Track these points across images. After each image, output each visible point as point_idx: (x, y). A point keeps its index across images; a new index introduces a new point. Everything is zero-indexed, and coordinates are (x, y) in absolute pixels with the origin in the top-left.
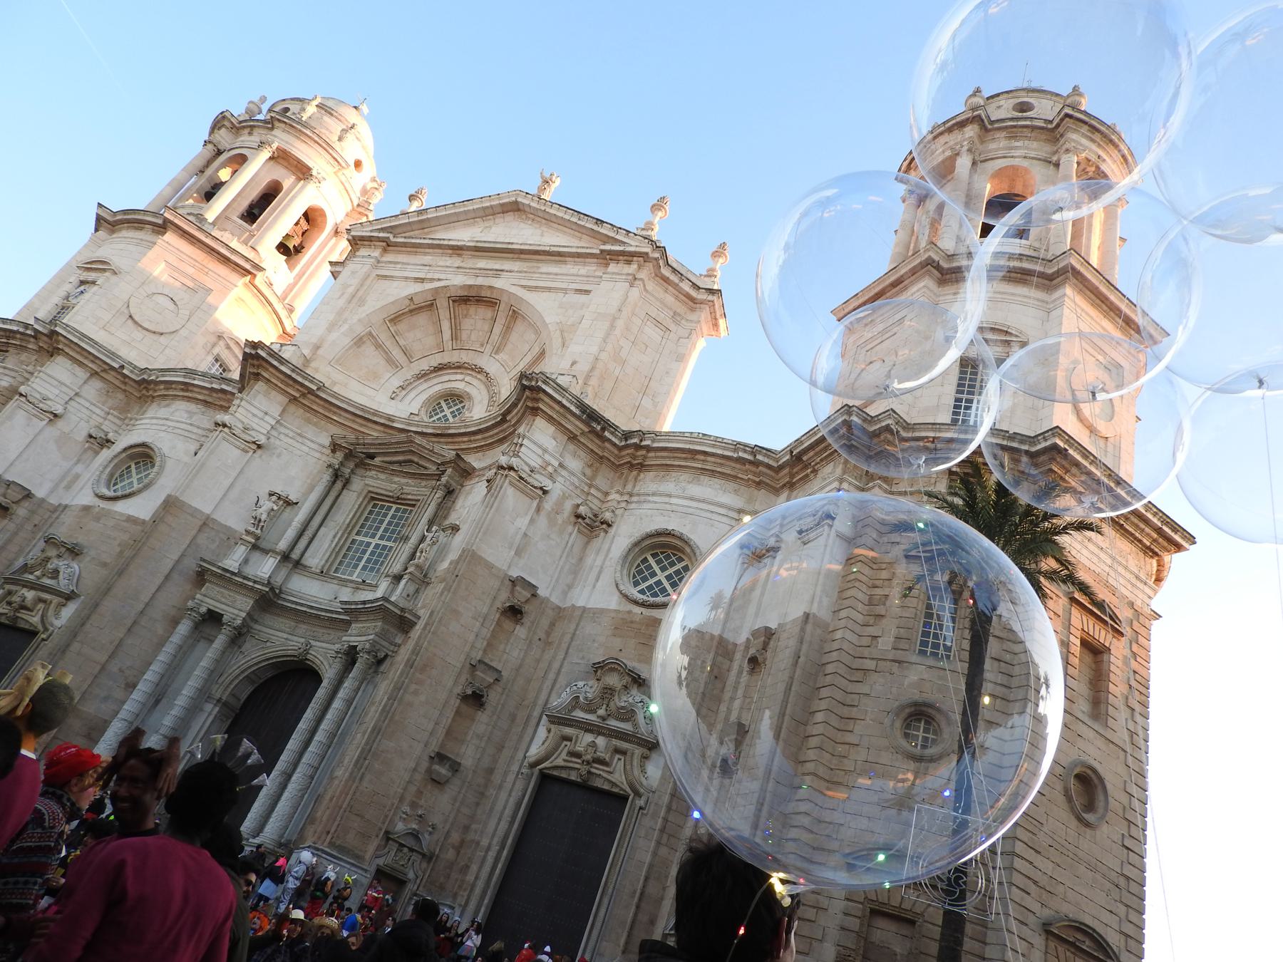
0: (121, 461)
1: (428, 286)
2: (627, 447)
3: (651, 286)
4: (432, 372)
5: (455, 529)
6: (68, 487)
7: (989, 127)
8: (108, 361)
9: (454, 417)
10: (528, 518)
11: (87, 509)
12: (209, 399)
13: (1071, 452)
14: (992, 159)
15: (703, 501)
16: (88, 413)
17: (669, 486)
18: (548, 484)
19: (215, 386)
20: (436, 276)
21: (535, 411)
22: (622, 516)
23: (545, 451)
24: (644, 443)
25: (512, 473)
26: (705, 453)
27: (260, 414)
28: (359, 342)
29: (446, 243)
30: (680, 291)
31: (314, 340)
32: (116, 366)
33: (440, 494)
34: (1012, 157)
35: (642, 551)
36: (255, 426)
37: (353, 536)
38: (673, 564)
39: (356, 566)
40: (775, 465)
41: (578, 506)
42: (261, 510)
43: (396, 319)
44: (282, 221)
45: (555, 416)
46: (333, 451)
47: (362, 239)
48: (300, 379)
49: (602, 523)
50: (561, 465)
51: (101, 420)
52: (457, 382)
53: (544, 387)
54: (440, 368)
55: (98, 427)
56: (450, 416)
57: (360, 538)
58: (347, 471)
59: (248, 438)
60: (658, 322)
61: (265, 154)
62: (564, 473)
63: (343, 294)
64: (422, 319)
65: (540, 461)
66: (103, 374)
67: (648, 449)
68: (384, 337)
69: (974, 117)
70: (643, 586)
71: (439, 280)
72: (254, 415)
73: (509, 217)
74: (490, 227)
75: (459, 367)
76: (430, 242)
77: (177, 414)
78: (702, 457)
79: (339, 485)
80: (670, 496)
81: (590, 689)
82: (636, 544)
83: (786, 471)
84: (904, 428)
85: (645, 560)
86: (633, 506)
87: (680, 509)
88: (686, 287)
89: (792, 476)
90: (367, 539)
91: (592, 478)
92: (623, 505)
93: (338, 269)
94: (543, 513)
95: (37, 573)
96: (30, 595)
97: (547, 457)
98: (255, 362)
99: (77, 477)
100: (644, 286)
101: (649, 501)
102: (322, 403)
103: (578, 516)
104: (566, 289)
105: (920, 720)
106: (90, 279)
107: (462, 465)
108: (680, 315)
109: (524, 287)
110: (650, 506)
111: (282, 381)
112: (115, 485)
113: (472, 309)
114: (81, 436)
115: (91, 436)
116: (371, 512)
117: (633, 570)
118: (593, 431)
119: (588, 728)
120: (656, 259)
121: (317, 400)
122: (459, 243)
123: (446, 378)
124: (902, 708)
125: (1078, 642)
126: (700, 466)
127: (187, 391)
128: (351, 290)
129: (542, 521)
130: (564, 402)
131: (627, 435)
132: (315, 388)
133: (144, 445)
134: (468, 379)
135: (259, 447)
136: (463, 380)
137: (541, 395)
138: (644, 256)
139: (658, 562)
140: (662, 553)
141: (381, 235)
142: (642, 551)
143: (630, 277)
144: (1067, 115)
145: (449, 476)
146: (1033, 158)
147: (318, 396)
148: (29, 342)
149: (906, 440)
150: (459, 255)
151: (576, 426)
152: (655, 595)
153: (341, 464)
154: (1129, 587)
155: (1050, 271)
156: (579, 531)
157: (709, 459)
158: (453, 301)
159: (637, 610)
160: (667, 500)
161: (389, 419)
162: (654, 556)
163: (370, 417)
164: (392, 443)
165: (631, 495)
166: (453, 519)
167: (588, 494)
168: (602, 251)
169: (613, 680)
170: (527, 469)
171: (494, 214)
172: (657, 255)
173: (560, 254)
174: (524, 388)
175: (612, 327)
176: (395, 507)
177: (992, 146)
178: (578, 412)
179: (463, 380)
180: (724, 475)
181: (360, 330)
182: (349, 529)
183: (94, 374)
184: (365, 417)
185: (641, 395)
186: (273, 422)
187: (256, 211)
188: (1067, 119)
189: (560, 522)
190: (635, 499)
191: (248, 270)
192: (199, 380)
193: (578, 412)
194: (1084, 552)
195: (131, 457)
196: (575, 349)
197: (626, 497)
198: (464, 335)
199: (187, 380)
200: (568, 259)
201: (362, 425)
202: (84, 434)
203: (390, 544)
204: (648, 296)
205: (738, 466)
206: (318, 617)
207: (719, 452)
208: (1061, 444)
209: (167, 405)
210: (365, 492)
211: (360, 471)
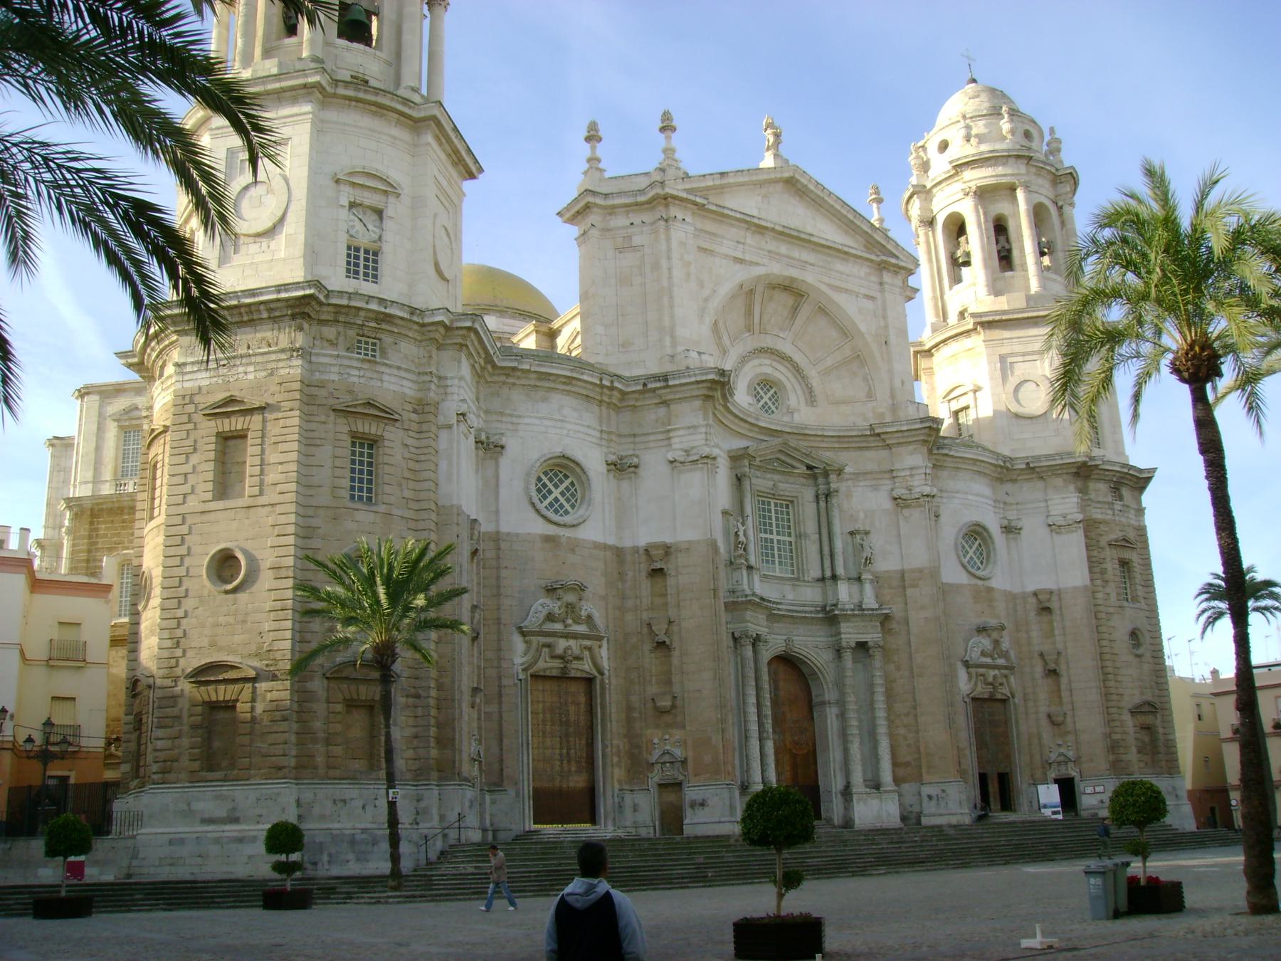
11: (548, 539)
20: (754, 259)
26: (983, 461)
29: (756, 221)
39: (773, 562)
63: (688, 275)
71: (757, 264)
80: (966, 493)
86: (945, 500)
89: (1019, 475)
96: (572, 643)
106: (367, 202)
109: (829, 286)
134: (774, 364)
148: (410, 329)
159: (980, 583)
161: (757, 419)
169: (995, 635)
173: (846, 253)
176: (772, 502)
179: (771, 366)
192: (589, 375)
199: (575, 375)
206: (792, 617)
209: (545, 400)
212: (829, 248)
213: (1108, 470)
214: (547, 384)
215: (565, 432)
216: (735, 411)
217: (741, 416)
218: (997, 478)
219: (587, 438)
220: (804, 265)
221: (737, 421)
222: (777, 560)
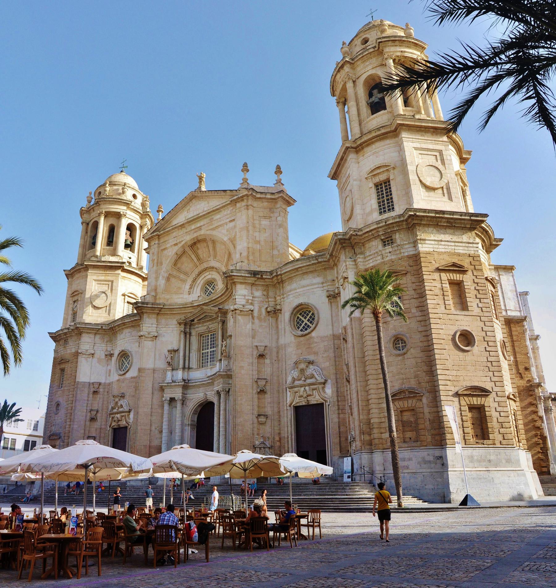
0: (119, 360)
1: (180, 245)
2: (273, 277)
3: (255, 204)
4: (198, 276)
5: (231, 336)
6: (109, 375)
7: (353, 62)
8: (97, 327)
9: (213, 290)
10: (251, 323)
12: (133, 325)
13: (418, 214)
14: (360, 76)
15: (308, 286)
16: (101, 347)
17: (294, 285)
18: (251, 307)
19: (132, 320)
20: (181, 240)
21: (234, 283)
22: (284, 304)
23: (245, 296)
24: (279, 273)
25: (237, 311)
27: (150, 325)
28: (168, 279)
29: (177, 225)
30: (268, 199)
31: (153, 288)
32: (100, 327)
33: (220, 325)
34: (368, 71)
35: (295, 315)
36: (151, 330)
37: (202, 352)
38: (308, 315)
39: (208, 362)
40: (326, 260)
41: (267, 308)
42: (168, 359)
43: (175, 264)
44: (122, 235)
45: (242, 281)
46: (180, 325)
47: (149, 238)
48: (156, 306)
49: (278, 310)
50: (253, 297)
51: (106, 348)
52: (208, 276)
53: (232, 274)
54: (200, 274)
55: (107, 351)
56: (212, 291)
57: (204, 351)
58: (188, 330)
59: (151, 336)
60: (265, 217)
61: (102, 219)
62: (256, 299)
64: (184, 259)
65: (245, 301)
66: (98, 332)
67: (281, 275)
68: (175, 273)
69: (344, 63)
70: (301, 327)
71: (182, 241)
72: (149, 327)
73: (194, 201)
74: (189, 209)
75: (205, 270)
76: (171, 228)
77: (126, 335)
78: (300, 269)
79: (188, 336)
80: (296, 289)
81: (295, 374)
82: (292, 313)
83: (331, 260)
84: (358, 231)
85: (298, 317)
87: (301, 293)
88: (269, 196)
90: (206, 351)
91: (268, 294)
92: (282, 300)
93: (148, 250)
94: (255, 318)
95: (117, 408)
97: (247, 298)
98: (140, 309)
99: (110, 371)
100: (253, 206)
101: (290, 295)
102: (167, 310)
103: (269, 312)
104: (226, 223)
105: (399, 341)
107: (223, 311)
108: (272, 208)
109: (212, 229)
110: (291, 296)
111: (151, 310)
112: (122, 368)
113: (198, 245)
114: (103, 357)
115: (106, 355)
116: (203, 340)
117: (296, 323)
118: (258, 278)
119: (301, 386)
120: (252, 194)
121: (165, 310)
122: (182, 223)
123: (203, 276)
124: (391, 339)
125: (448, 285)
126: (301, 273)
127: (125, 325)
128: (155, 261)
129: (256, 321)
130: (243, 275)
131: (271, 273)
132: (162, 306)
133: (123, 351)
134: (211, 272)
135: (156, 337)
136: (209, 274)
137: (233, 277)
138: (247, 195)
139: (303, 316)
140: (303, 312)
141: (155, 234)
142: (295, 315)
143: (245, 207)
144: (379, 42)
145: (220, 317)
146: (376, 67)
147: (165, 308)
149: (361, 235)
150: (184, 227)
151: (251, 280)
152: (306, 329)
153: (185, 328)
154: (466, 249)
155: (393, 128)
156: (271, 317)
157: (303, 268)
158: (191, 246)
160: (295, 291)
161: (192, 304)
162: (300, 314)
163: (185, 306)
164: (197, 313)
165: (283, 295)
166: (229, 334)
167: (269, 301)
168: (231, 201)
170: (241, 306)
171: (188, 203)
172: (250, 193)
173: (217, 209)
174: (226, 277)
175: (248, 231)
176: (210, 334)
177: (359, 69)
178: (249, 275)
179: (209, 274)
180: (311, 272)
181: (166, 275)
182: (199, 350)
183: (95, 334)
184: (184, 307)
185: (272, 251)
186: (156, 326)
187: (111, 240)
188: (380, 44)
189: (263, 318)
190: (285, 296)
191: (120, 267)
193: (249, 275)
194: (440, 247)
195: (121, 357)
196: (239, 247)
197: (282, 297)
198: (201, 256)
199: (123, 322)
200: (221, 209)
201: (184, 310)
202: (104, 355)
203: (214, 349)
204: (256, 209)
205: (314, 266)
207: (305, 265)
208: (412, 213)
209: (122, 333)
210: (197, 334)
211: (192, 327)
212: (209, 213)
213: (367, 232)
214: (120, 328)
215: (125, 342)
216: (175, 307)
217: (182, 307)
218: (325, 269)
219: (133, 340)
220: (200, 228)
221: (182, 309)
222: (209, 360)
